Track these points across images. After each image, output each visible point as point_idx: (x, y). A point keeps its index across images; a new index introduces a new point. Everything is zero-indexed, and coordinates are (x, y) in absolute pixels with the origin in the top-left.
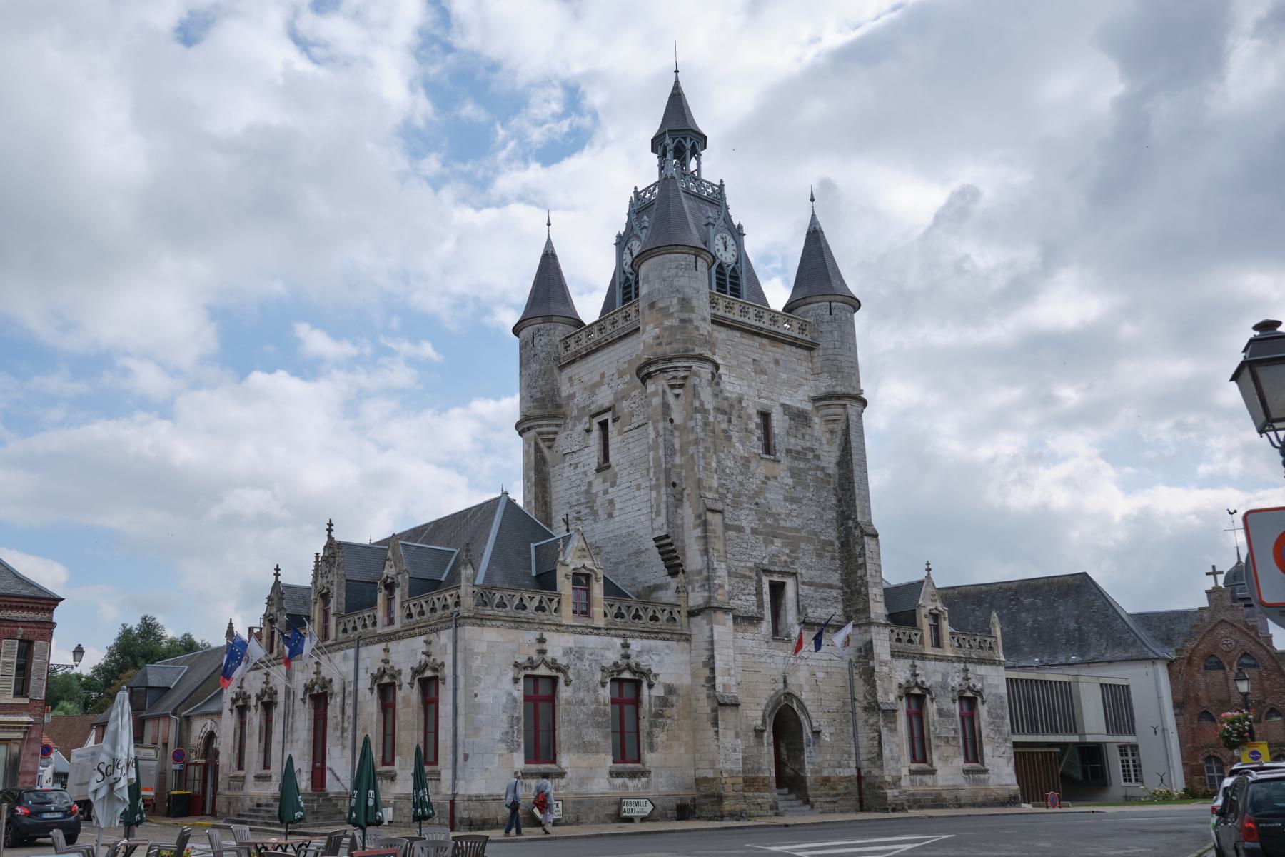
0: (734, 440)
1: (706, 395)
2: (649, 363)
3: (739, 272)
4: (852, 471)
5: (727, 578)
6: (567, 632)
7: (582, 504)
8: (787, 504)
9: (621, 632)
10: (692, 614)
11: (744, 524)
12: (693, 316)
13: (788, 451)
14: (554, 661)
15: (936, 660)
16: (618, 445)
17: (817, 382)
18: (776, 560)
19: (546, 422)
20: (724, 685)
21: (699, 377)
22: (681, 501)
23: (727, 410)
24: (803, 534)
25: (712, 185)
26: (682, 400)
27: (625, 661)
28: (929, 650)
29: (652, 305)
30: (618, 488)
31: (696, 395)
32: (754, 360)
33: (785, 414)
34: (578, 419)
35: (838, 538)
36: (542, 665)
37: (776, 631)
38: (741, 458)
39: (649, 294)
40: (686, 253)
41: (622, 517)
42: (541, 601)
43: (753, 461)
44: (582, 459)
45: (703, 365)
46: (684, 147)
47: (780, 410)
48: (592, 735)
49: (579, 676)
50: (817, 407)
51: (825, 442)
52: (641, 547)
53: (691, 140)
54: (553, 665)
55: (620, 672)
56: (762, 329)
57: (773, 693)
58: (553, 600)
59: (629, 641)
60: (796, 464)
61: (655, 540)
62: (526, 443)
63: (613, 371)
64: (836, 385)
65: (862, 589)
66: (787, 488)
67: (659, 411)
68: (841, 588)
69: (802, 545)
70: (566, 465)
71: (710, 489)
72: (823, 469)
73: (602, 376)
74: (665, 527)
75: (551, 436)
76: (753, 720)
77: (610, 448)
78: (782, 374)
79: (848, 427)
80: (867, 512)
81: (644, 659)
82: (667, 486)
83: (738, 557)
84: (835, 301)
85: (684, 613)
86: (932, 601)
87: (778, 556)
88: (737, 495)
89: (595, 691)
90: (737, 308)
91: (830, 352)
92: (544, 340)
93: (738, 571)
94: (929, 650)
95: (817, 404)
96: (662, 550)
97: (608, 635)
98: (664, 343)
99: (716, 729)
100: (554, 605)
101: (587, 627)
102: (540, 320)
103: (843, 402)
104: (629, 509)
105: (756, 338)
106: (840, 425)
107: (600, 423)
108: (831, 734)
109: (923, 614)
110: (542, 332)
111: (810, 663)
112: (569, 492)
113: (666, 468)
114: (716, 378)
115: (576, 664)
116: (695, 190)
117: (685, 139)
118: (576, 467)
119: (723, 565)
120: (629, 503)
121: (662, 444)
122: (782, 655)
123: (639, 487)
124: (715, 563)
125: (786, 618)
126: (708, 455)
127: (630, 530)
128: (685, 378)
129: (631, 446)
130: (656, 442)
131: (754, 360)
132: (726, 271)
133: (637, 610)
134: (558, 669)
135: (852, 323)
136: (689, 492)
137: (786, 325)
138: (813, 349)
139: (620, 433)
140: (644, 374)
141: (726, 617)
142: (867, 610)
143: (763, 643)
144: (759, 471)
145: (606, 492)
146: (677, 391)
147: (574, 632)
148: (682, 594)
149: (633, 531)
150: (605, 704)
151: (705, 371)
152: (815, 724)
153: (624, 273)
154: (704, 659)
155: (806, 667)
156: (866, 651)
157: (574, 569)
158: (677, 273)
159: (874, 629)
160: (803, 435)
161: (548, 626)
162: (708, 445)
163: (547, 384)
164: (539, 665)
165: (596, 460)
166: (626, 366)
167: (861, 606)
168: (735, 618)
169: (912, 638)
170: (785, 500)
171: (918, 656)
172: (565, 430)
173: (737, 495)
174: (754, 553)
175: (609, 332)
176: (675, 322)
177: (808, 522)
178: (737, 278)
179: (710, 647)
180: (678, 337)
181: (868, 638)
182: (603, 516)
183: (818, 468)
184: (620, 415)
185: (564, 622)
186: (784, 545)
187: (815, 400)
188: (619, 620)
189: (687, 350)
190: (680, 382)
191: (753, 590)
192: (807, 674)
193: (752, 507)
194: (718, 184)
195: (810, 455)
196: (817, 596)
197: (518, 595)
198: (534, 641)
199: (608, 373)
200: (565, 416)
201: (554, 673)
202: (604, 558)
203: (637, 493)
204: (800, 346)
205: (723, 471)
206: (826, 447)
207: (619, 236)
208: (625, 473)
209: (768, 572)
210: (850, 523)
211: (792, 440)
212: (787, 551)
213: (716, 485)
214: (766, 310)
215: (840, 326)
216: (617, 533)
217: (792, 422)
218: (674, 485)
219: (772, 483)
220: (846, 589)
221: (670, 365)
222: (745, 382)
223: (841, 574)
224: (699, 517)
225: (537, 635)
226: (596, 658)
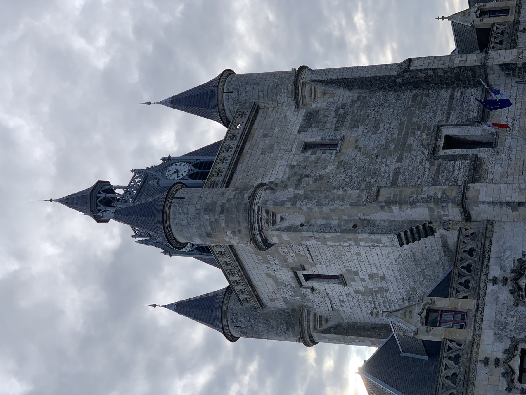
0: (323, 173)
1: (282, 195)
2: (254, 240)
3: (196, 162)
4: (356, 79)
5: (438, 187)
6: (479, 336)
7: (373, 299)
8: (379, 131)
9: (482, 285)
10: (468, 218)
11: (393, 168)
12: (219, 202)
13: (336, 129)
14: (506, 351)
15: (519, 12)
16: (324, 267)
17: (284, 104)
18: (425, 142)
19: (306, 323)
21: (267, 201)
22: (369, 221)
23: (299, 177)
24: (405, 119)
25: (134, 178)
26: (286, 215)
27: (509, 282)
28: (511, 18)
29: (209, 235)
30: (360, 270)
31: (282, 203)
32: (262, 154)
33: (307, 131)
34: (303, 296)
35: (411, 90)
36: (510, 363)
37: (489, 145)
38: (338, 168)
39: (201, 237)
40: (170, 205)
41: (384, 269)
42: (450, 358)
43: (341, 158)
44: (336, 296)
45: (258, 197)
46: (104, 198)
47: (303, 134)
50: (304, 105)
51: (332, 100)
52: (409, 255)
53: (99, 193)
54: (510, 352)
56: (238, 147)
58: (449, 346)
59: (490, 277)
60: (347, 123)
61: (402, 245)
62: (322, 339)
63: (264, 267)
64: (287, 89)
65: (455, 71)
66: (366, 131)
67: (293, 235)
68: (454, 89)
69: (414, 120)
70: (341, 309)
71: (359, 196)
72: (353, 102)
73: (268, 275)
74: (391, 236)
75: (318, 319)
77: (326, 274)
78: (275, 132)
79: (320, 81)
80: (390, 67)
81: (508, 265)
82: (355, 232)
83: (421, 174)
84: (223, 89)
85: (468, 225)
86: (469, 15)
87: (422, 141)
88: (369, 173)
90: (220, 166)
91: (261, 93)
92: (240, 319)
94: (511, 18)
95: (301, 105)
96: (410, 239)
98: (239, 228)
100: (454, 345)
101: (475, 316)
102: (225, 320)
103: (301, 84)
104: (377, 263)
105: (244, 151)
106: (319, 87)
109: (480, 23)
110: (234, 320)
112: (364, 308)
113: (341, 232)
114: (272, 186)
116: (135, 192)
117: (98, 197)
118: (343, 301)
119: (425, 189)
120: (372, 262)
121: (321, 235)
122: (509, 140)
123: (358, 254)
124: (423, 196)
125: (477, 136)
126: (331, 197)
127: (394, 263)
128: (267, 212)
129: (324, 258)
130: (319, 239)
131: (262, 154)
132: (195, 171)
133: (463, 267)
134: (516, 349)
135: (238, 75)
136: (362, 214)
137: (238, 127)
138: (258, 106)
139: (314, 266)
140: (266, 245)
141: (471, 189)
142: (472, 68)
143: (498, 156)
144: (350, 154)
145: (363, 280)
146: (278, 219)
147: (480, 329)
148: (450, 226)
149: (396, 261)
151: (263, 195)
153: (192, 251)
154: (510, 211)
156: (509, 69)
157: (422, 323)
158: (185, 213)
159: (490, 63)
160: (325, 116)
161: (474, 354)
162: (323, 196)
163: (275, 319)
164: (510, 367)
165: (336, 286)
167: (470, 73)
168: (474, 180)
169: (500, 31)
170: (375, 133)
171: (515, 27)
172: (313, 308)
173: (369, 173)
175: (233, 268)
176: (223, 217)
177: (396, 114)
178: (201, 163)
180: (234, 216)
181: (497, 67)
182: (383, 284)
183: (352, 106)
184: (299, 265)
185: (470, 338)
186: (414, 135)
187: (297, 106)
188: (471, 285)
189: (245, 210)
190: (271, 216)
191: (449, 164)
193: (379, 160)
194: (134, 173)
195: (342, 111)
196: (458, 108)
197: (442, 380)
198: (487, 369)
199: (266, 271)
200: (302, 307)
201: (518, 353)
202: (419, 286)
203: (364, 256)
204: (255, 116)
205: (347, 183)
206: (336, 98)
207: (165, 253)
208: (347, 264)
209: (434, 151)
210: (399, 80)
211: (328, 126)
212: (419, 133)
213: (357, 191)
214: (224, 142)
215: (242, 86)
216: (397, 274)
217: (314, 125)
218: (355, 226)
219: (361, 143)
220: (455, 85)
221: (256, 224)
222: (278, 162)
223: (442, 88)
224: (382, 208)
225: (480, 366)
226: (505, 310)
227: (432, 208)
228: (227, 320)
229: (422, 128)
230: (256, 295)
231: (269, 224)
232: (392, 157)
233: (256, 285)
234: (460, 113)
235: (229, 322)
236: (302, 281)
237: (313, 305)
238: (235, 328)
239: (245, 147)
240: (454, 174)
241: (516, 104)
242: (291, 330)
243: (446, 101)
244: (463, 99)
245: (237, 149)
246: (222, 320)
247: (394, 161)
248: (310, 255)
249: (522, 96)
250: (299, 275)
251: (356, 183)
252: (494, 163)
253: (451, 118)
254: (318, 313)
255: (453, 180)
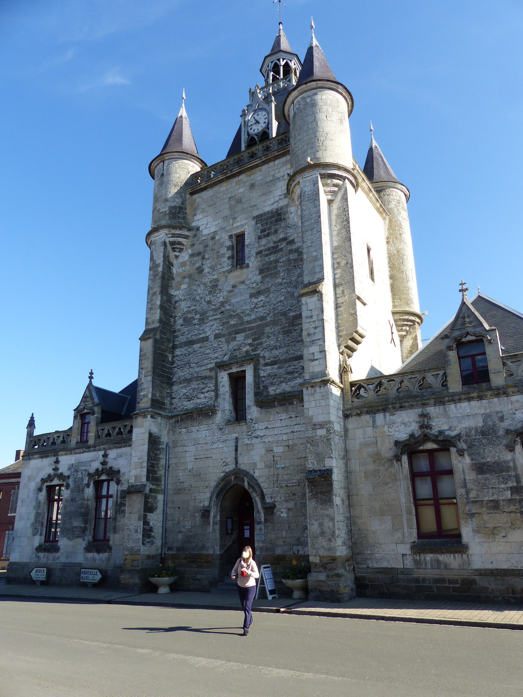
9: (102, 447)
18: (237, 353)
20: (136, 477)
48: (77, 523)
49: (75, 481)
55: (99, 476)
57: (222, 475)
76: (200, 502)
89: (83, 491)
93: (199, 375)
97: (95, 451)
108: (289, 510)
111: (266, 440)
115: (74, 475)
141: (144, 420)
150: (88, 500)
152: (268, 500)
155: (262, 445)
164: (54, 479)
174: (216, 355)
186: (247, 337)
192: (263, 451)
193: (217, 317)
229: (255, 343)
232: (221, 328)
234: (276, 375)
239: (239, 176)
240: (200, 394)
241: (286, 433)
243: (294, 354)
244: (297, 372)
245: (229, 172)
247: (217, 331)
249: (297, 438)
251: (193, 308)
252: (210, 429)
253: (268, 367)
255: (194, 395)
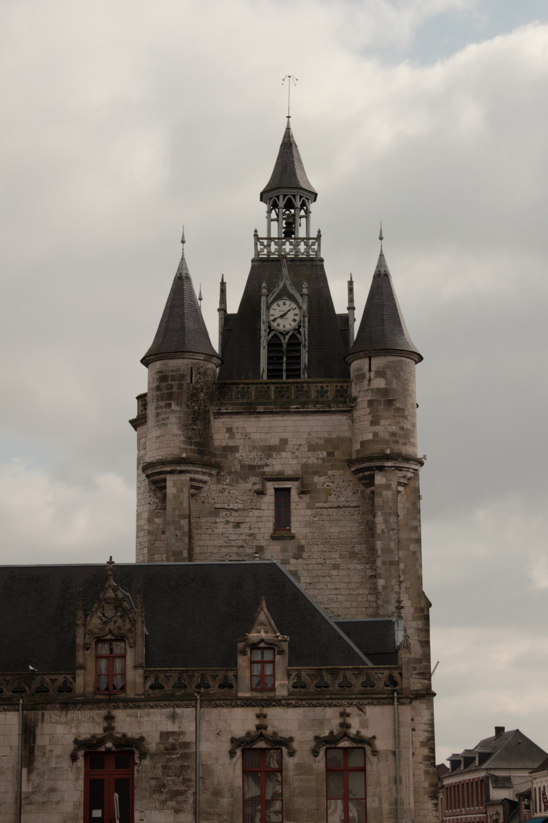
44: (248, 520)
73: (284, 442)
75: (201, 485)
99: (436, 801)
102: (202, 357)
107: (276, 490)
112: (224, 550)
120: (322, 580)
123: (336, 567)
128: (409, 479)
136: (408, 586)
139: (309, 507)
146: (401, 489)
154: (421, 739)
166: (322, 442)
179: (430, 729)
199: (292, 442)
203: (334, 572)
208: (316, 549)
227: (422, 663)
228: (200, 360)
230: (244, 412)
231: (401, 479)
233: (262, 419)
235: (198, 361)
236: (277, 484)
237: (224, 485)
238: (190, 368)
242: (193, 447)
246: (204, 354)
248: (330, 508)
250: (287, 482)
254: (208, 487)
